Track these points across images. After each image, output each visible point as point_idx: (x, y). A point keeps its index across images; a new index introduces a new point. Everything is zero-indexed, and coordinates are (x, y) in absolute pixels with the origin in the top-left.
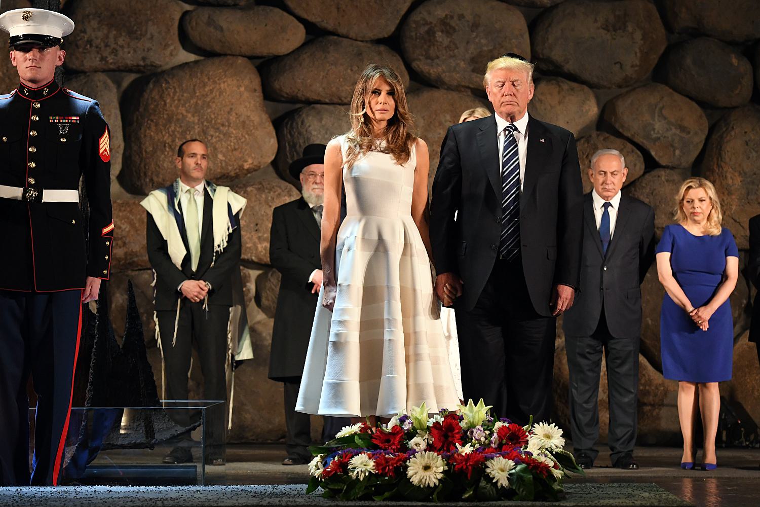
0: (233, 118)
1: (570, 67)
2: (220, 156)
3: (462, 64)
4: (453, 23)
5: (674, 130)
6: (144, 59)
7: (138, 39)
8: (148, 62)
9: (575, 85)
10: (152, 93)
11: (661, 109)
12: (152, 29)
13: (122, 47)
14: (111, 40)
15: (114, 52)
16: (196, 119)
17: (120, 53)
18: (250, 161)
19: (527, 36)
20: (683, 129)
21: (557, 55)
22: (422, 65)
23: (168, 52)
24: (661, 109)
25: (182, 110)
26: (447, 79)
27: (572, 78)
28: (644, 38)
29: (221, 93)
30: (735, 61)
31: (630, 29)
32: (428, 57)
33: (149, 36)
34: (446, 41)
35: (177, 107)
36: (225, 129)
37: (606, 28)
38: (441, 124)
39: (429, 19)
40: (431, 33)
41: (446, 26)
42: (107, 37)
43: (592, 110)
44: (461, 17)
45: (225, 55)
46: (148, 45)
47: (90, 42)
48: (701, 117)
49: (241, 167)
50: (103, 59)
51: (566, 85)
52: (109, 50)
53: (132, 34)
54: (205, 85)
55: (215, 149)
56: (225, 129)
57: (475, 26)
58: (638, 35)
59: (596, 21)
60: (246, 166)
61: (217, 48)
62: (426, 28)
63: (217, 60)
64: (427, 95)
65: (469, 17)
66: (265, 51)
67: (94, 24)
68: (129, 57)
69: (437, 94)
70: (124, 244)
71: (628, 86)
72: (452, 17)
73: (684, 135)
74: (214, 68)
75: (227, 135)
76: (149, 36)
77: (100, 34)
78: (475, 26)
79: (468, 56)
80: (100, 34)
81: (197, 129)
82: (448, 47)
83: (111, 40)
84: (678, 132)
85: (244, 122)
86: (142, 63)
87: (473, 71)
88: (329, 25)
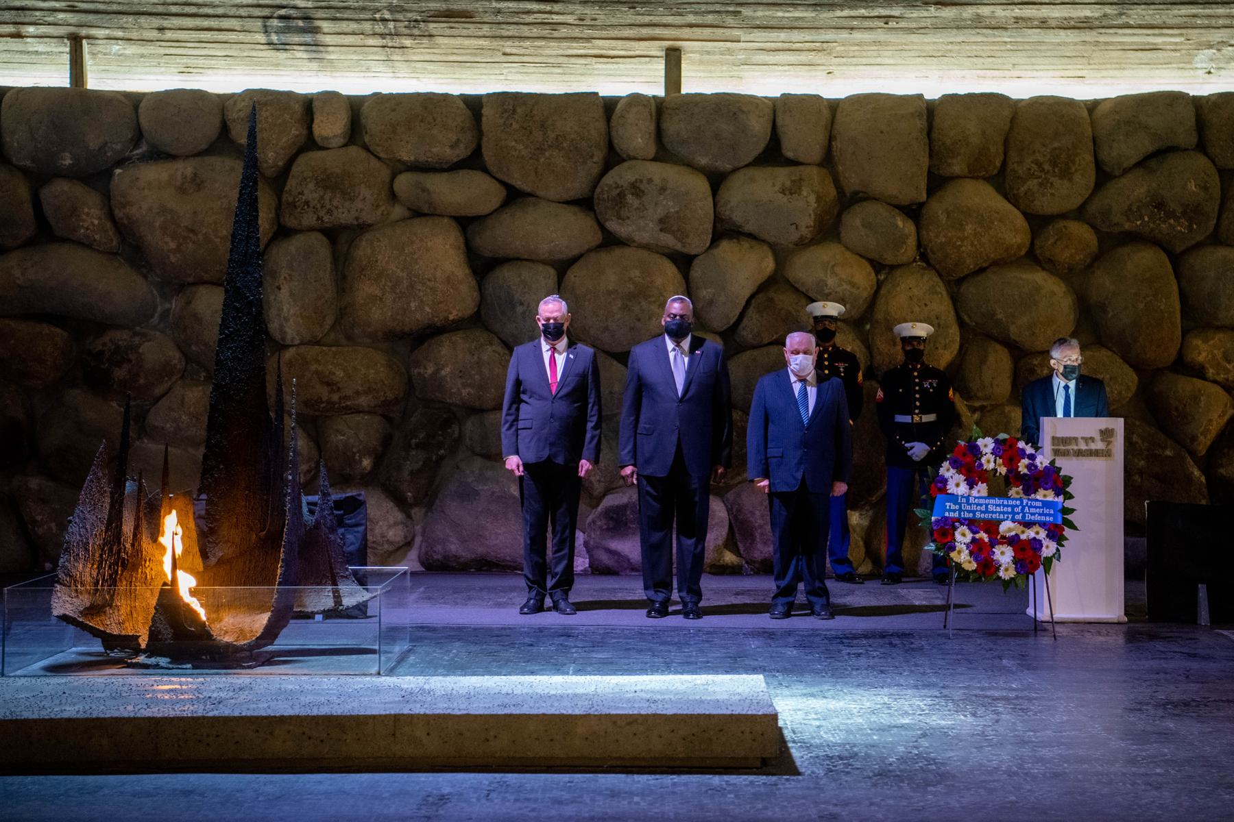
0: (439, 274)
1: (749, 228)
2: (427, 309)
3: (651, 225)
4: (642, 187)
5: (845, 286)
6: (357, 219)
7: (352, 200)
8: (361, 221)
9: (753, 243)
10: (363, 249)
11: (833, 266)
12: (364, 191)
13: (337, 208)
14: (327, 202)
15: (330, 212)
16: (405, 275)
17: (335, 213)
18: (455, 313)
19: (710, 199)
20: (853, 285)
21: (737, 217)
22: (613, 225)
23: (379, 212)
24: (833, 266)
25: (393, 267)
26: (636, 238)
27: (752, 236)
28: (819, 199)
29: (428, 250)
30: (900, 224)
31: (805, 193)
32: (619, 218)
33: (361, 197)
34: (636, 203)
35: (387, 263)
36: (431, 284)
37: (783, 192)
38: (630, 279)
39: (620, 183)
40: (621, 195)
41: (636, 189)
42: (322, 198)
43: (769, 265)
44: (650, 181)
45: (432, 215)
46: (360, 205)
47: (307, 203)
48: (870, 274)
49: (446, 318)
50: (318, 219)
51: (746, 244)
52: (325, 210)
53: (349, 197)
54: (413, 243)
55: (422, 301)
56: (431, 284)
57: (663, 190)
58: (812, 199)
59: (774, 185)
60: (451, 317)
61: (425, 209)
62: (618, 191)
63: (423, 219)
64: (618, 252)
65: (657, 180)
66: (471, 212)
67: (311, 186)
68: (344, 215)
69: (627, 251)
70: (339, 389)
71: (803, 244)
72: (641, 181)
73: (854, 290)
74: (420, 228)
75: (433, 290)
76: (361, 197)
77: (316, 196)
78: (663, 190)
79: (656, 217)
80: (316, 196)
81: (406, 283)
82: (637, 208)
83: (327, 202)
84: (848, 287)
85: (448, 279)
86: (355, 222)
87: (661, 230)
88: (527, 188)
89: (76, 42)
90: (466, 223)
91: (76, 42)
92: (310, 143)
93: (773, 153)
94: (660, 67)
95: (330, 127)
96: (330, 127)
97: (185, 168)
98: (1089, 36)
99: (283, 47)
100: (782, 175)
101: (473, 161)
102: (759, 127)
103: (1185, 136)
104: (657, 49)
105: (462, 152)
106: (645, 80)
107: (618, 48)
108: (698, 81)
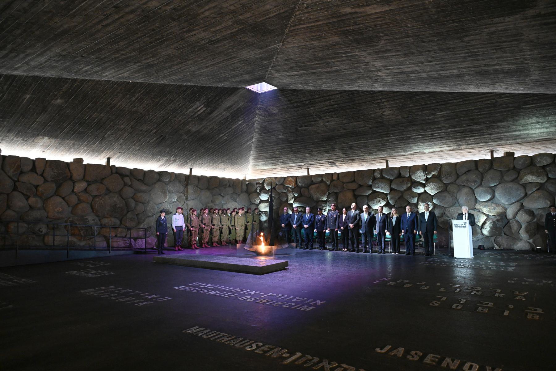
89: (308, 169)
90: (354, 191)
91: (308, 169)
92: (332, 180)
93: (399, 176)
94: (385, 164)
95: (335, 178)
96: (335, 178)
97: (318, 185)
98: (457, 151)
99: (333, 166)
100: (401, 180)
101: (354, 181)
102: (396, 172)
103: (473, 167)
104: (384, 161)
105: (352, 180)
106: (382, 166)
107: (378, 161)
108: (391, 165)
